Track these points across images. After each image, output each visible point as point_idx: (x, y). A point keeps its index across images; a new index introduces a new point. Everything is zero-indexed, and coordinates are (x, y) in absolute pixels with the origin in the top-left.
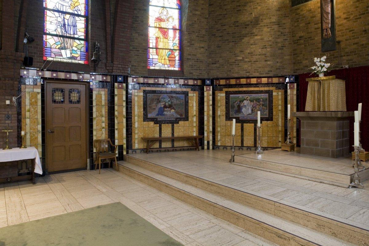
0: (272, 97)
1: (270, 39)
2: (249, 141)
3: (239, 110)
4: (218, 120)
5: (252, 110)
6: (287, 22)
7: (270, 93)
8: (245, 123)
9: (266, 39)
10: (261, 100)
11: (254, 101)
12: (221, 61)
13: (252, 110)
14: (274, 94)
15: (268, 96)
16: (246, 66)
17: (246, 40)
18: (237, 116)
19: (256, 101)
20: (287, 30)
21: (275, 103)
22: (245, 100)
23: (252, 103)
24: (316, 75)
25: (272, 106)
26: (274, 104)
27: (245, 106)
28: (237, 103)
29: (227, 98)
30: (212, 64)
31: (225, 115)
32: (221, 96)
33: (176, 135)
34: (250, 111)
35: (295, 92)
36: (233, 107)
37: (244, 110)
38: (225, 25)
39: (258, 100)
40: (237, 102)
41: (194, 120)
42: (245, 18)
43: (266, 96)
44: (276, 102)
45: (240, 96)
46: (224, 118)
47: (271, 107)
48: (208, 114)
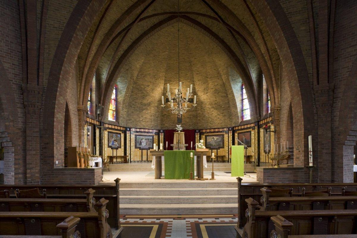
1: (154, 113)
2: (145, 158)
3: (141, 144)
4: (132, 148)
7: (153, 136)
9: (152, 112)
12: (133, 119)
14: (154, 137)
16: (143, 123)
17: (144, 111)
18: (140, 147)
20: (160, 110)
23: (146, 141)
24: (178, 131)
27: (143, 142)
29: (136, 138)
30: (129, 120)
33: (117, 155)
35: (163, 137)
36: (138, 142)
37: (143, 144)
38: (136, 103)
39: (148, 139)
41: (123, 147)
42: (145, 101)
43: (151, 138)
45: (141, 137)
46: (134, 147)
48: (128, 145)
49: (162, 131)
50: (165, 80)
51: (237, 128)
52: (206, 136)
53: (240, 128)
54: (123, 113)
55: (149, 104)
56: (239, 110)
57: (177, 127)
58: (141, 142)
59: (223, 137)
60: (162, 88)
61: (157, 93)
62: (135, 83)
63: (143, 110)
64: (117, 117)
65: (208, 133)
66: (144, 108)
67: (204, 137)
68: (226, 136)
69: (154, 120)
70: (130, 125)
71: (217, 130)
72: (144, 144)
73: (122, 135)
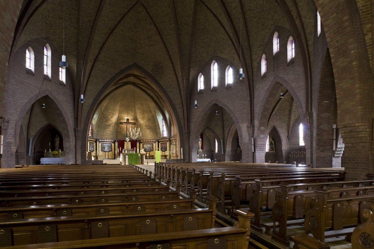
6: (116, 126)
7: (111, 144)
12: (100, 134)
17: (106, 129)
24: (127, 141)
29: (102, 145)
32: (100, 144)
39: (109, 146)
42: (107, 124)
49: (116, 141)
50: (119, 112)
51: (160, 140)
52: (143, 144)
53: (161, 140)
54: (95, 131)
55: (109, 125)
56: (161, 130)
57: (126, 139)
58: (104, 147)
59: (153, 145)
60: (117, 115)
61: (114, 119)
62: (102, 114)
63: (106, 129)
64: (92, 134)
65: (144, 142)
66: (107, 127)
67: (142, 144)
68: (154, 144)
69: (112, 134)
70: (98, 138)
71: (149, 141)
72: (106, 149)
73: (95, 144)
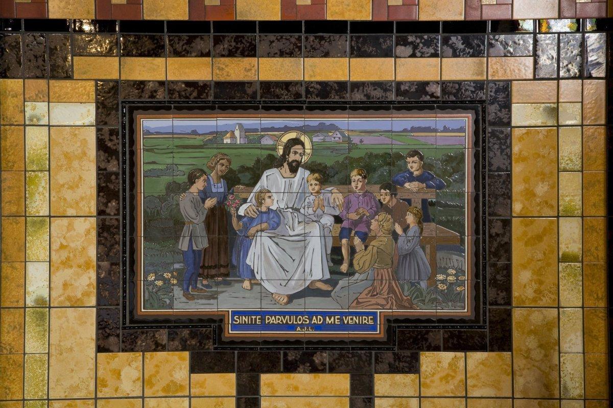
0: (506, 143)
3: (221, 252)
5: (335, 256)
8: (273, 369)
10: (414, 165)
11: (355, 176)
13: (336, 250)
15: (466, 140)
18: (200, 307)
19: (367, 171)
21: (530, 194)
22: (273, 162)
23: (335, 196)
25: (507, 223)
26: (517, 207)
27: (273, 221)
28: (205, 194)
29: (116, 145)
31: (93, 301)
34: (316, 268)
36: (169, 227)
37: (260, 253)
39: (383, 168)
40: (199, 185)
44: (541, 189)
45: (233, 127)
47: (497, 228)
